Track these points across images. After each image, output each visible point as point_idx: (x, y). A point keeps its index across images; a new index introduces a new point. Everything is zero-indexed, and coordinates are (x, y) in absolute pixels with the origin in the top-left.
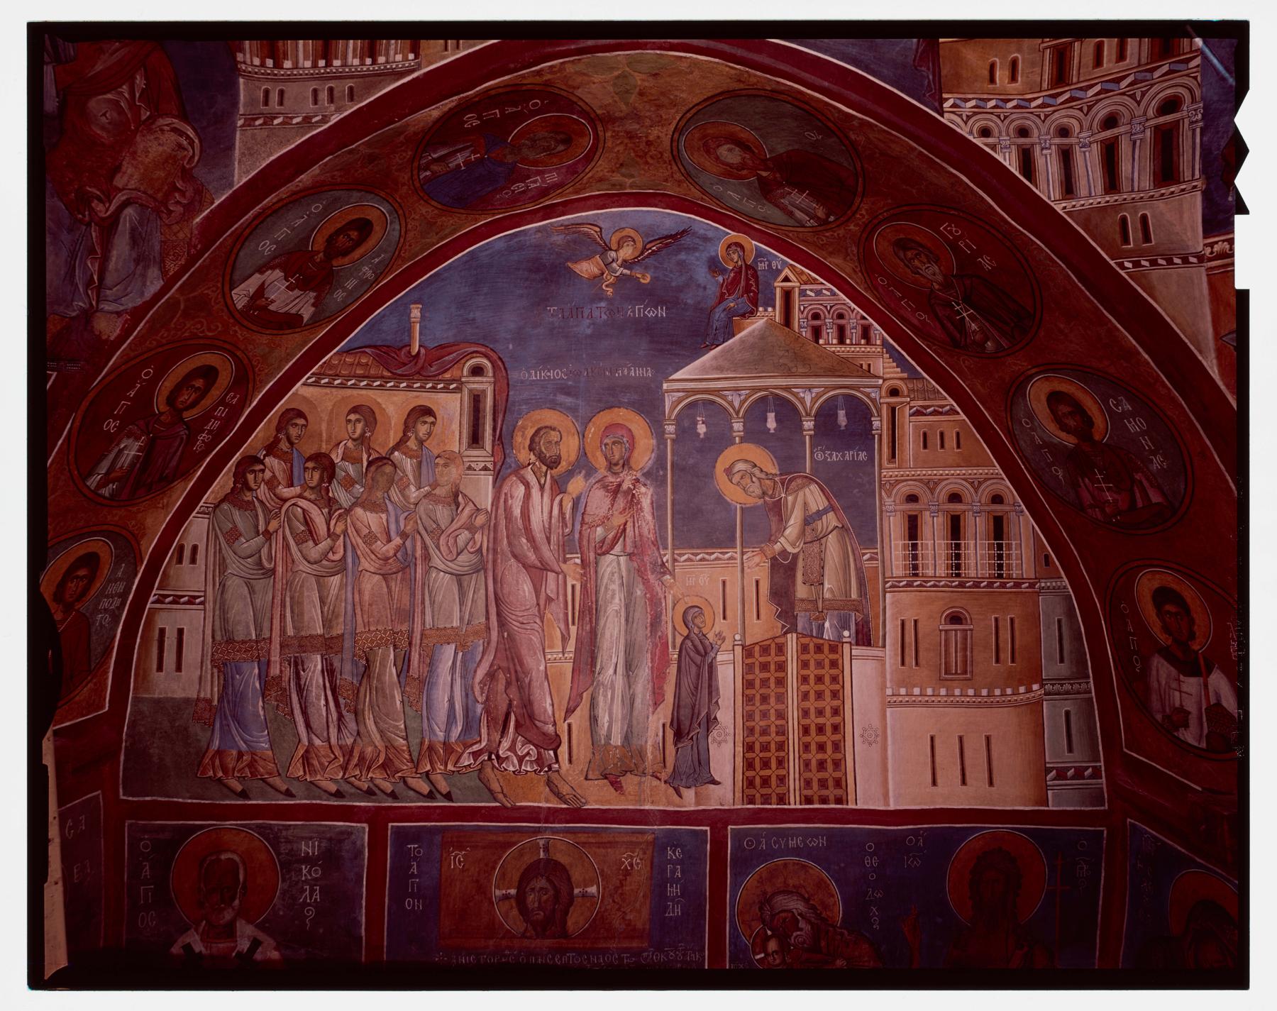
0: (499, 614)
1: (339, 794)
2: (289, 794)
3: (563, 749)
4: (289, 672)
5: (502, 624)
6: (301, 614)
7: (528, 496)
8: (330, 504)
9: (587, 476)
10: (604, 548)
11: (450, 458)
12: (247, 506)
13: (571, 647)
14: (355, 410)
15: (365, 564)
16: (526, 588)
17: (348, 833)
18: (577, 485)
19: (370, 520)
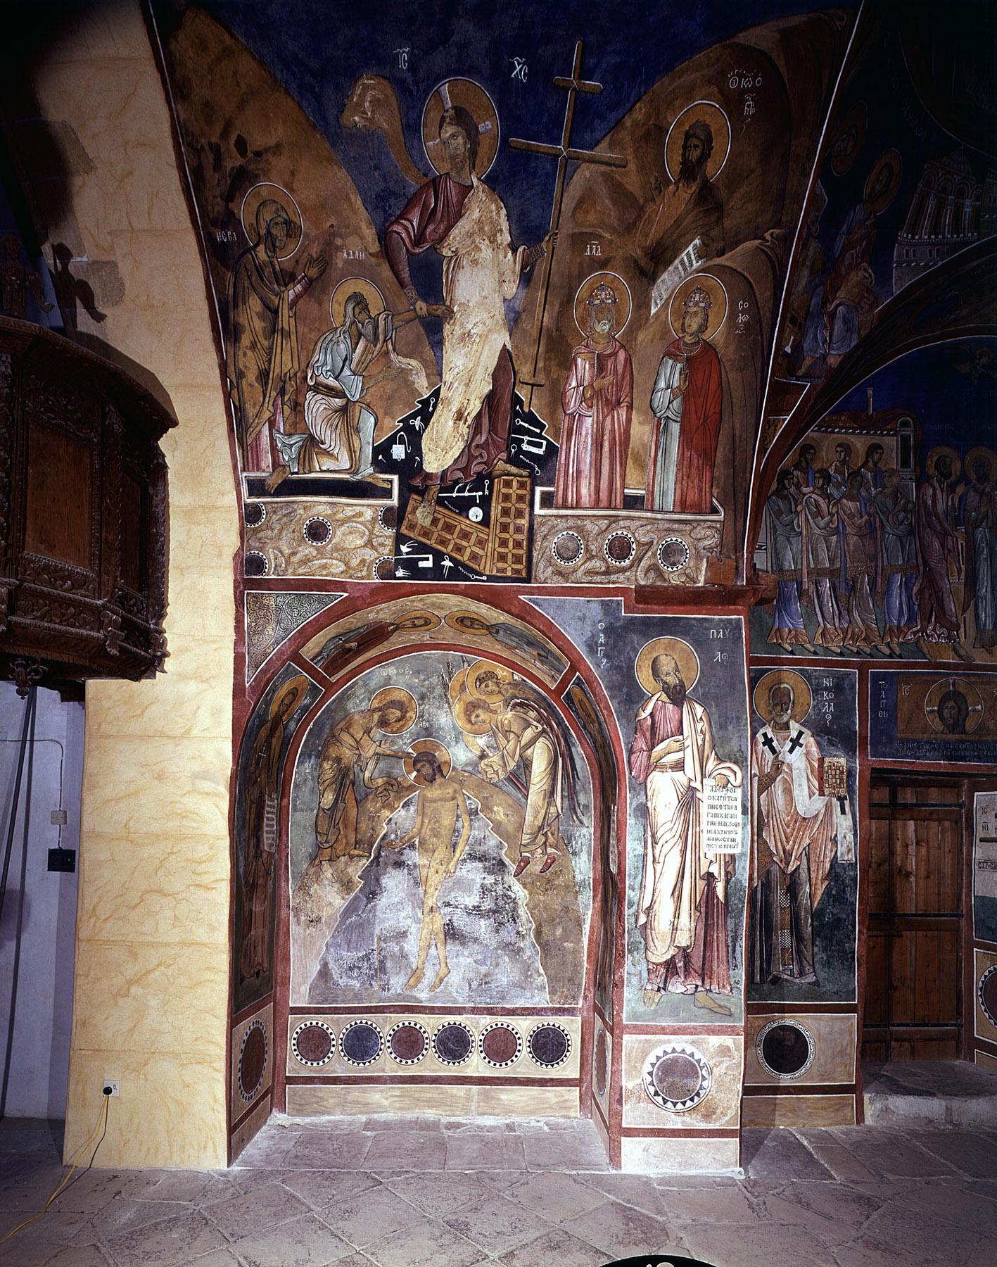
0: (923, 558)
1: (841, 654)
2: (815, 653)
3: (962, 629)
4: (812, 587)
5: (925, 563)
6: (817, 556)
7: (934, 494)
8: (828, 497)
9: (966, 485)
10: (977, 524)
11: (892, 472)
12: (785, 498)
13: (963, 577)
14: (839, 445)
15: (849, 530)
16: (937, 544)
17: (848, 674)
18: (960, 489)
19: (851, 505)
